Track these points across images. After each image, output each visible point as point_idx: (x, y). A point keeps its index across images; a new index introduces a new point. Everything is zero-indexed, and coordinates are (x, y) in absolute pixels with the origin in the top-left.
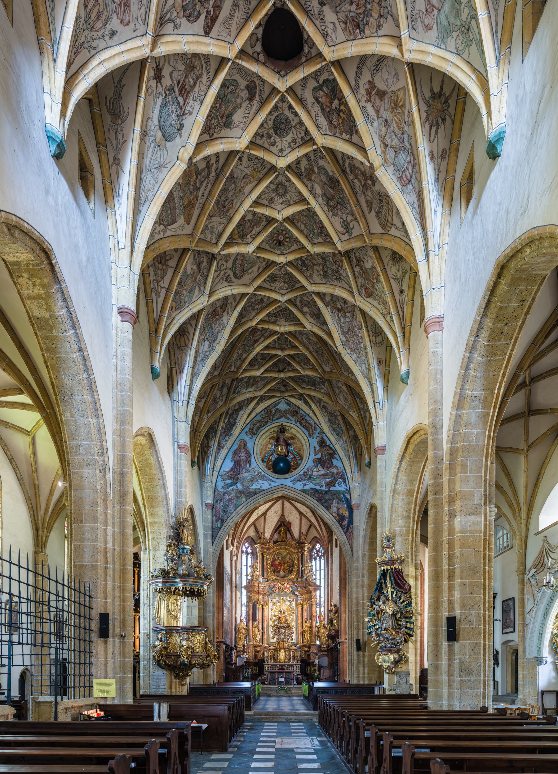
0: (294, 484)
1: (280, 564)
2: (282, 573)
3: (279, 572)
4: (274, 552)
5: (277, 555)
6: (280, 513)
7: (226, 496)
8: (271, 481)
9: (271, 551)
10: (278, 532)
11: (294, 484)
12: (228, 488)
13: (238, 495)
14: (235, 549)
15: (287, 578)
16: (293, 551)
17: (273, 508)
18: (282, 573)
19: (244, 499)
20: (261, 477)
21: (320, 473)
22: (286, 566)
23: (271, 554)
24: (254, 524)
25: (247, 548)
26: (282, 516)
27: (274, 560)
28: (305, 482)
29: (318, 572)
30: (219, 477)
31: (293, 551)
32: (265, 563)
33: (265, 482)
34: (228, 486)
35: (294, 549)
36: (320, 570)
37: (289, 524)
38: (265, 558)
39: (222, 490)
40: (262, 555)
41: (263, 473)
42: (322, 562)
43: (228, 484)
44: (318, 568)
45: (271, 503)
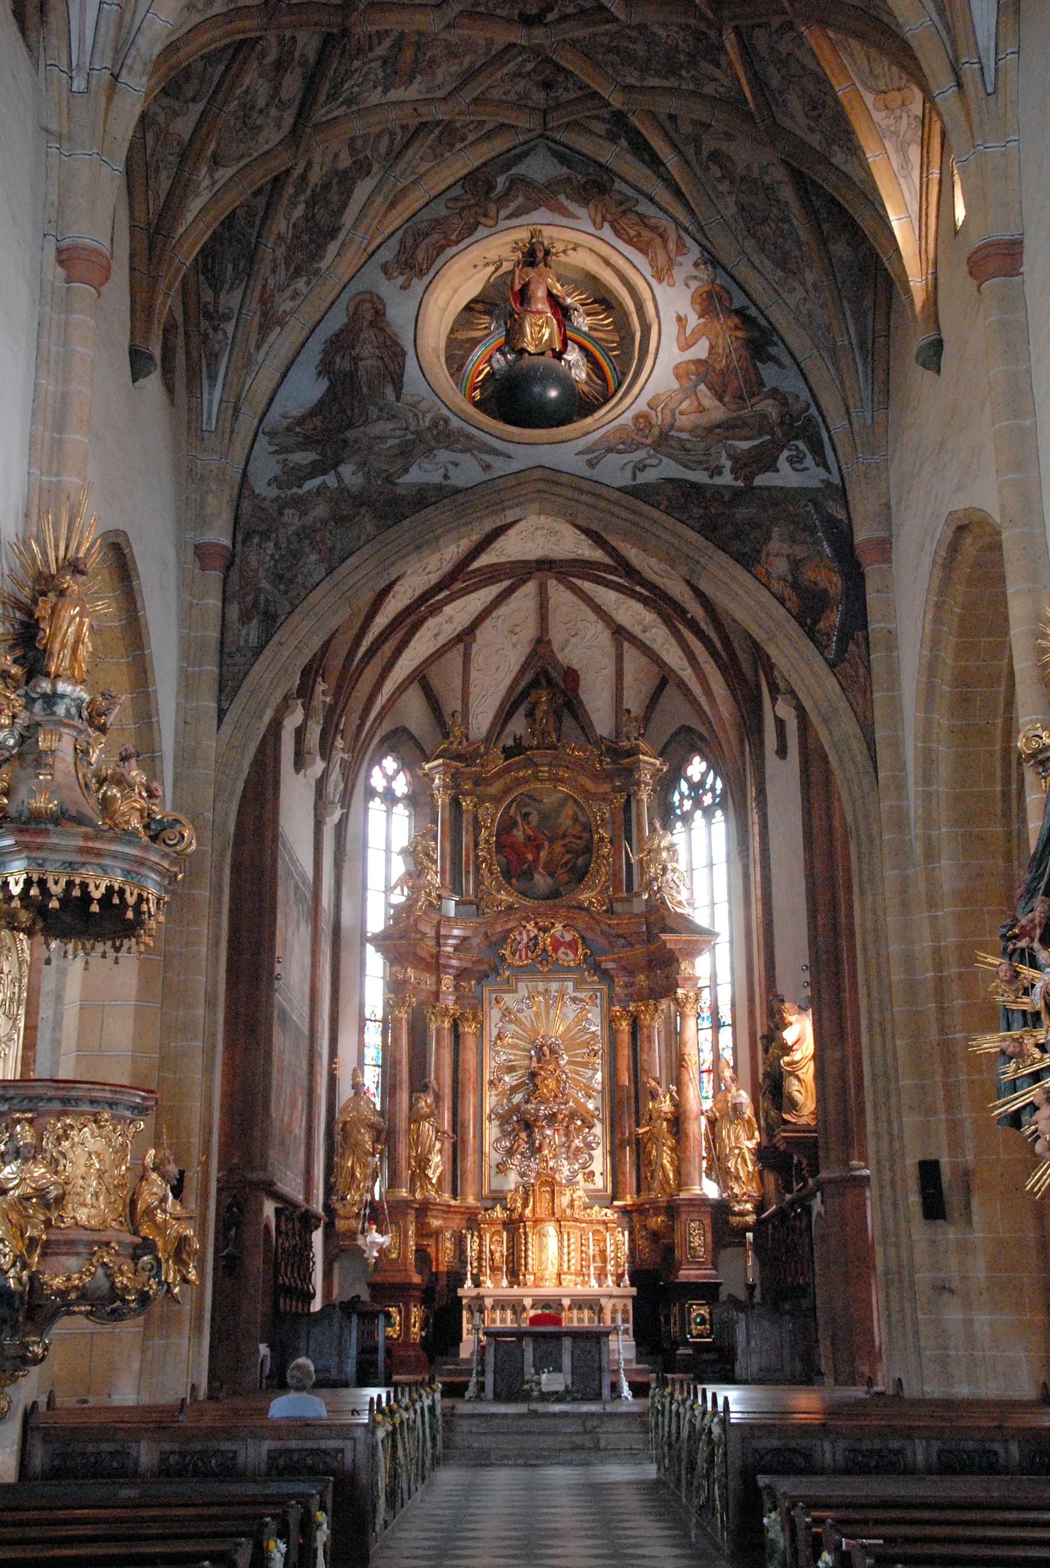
0: (591, 464)
2: (541, 881)
3: (528, 875)
4: (507, 791)
5: (520, 802)
6: (529, 632)
7: (290, 516)
9: (493, 790)
10: (522, 711)
11: (591, 464)
12: (300, 482)
13: (346, 510)
14: (335, 776)
15: (564, 901)
16: (589, 785)
17: (503, 610)
18: (541, 881)
19: (370, 528)
21: (704, 420)
22: (558, 849)
23: (496, 800)
24: (420, 677)
25: (390, 779)
26: (541, 643)
27: (506, 827)
28: (641, 454)
29: (701, 877)
30: (263, 440)
31: (589, 785)
32: (466, 839)
33: (465, 459)
34: (299, 475)
35: (595, 777)
36: (711, 865)
37: (572, 676)
38: (466, 820)
39: (272, 492)
40: (455, 803)
43: (299, 467)
44: (700, 860)
45: (494, 590)
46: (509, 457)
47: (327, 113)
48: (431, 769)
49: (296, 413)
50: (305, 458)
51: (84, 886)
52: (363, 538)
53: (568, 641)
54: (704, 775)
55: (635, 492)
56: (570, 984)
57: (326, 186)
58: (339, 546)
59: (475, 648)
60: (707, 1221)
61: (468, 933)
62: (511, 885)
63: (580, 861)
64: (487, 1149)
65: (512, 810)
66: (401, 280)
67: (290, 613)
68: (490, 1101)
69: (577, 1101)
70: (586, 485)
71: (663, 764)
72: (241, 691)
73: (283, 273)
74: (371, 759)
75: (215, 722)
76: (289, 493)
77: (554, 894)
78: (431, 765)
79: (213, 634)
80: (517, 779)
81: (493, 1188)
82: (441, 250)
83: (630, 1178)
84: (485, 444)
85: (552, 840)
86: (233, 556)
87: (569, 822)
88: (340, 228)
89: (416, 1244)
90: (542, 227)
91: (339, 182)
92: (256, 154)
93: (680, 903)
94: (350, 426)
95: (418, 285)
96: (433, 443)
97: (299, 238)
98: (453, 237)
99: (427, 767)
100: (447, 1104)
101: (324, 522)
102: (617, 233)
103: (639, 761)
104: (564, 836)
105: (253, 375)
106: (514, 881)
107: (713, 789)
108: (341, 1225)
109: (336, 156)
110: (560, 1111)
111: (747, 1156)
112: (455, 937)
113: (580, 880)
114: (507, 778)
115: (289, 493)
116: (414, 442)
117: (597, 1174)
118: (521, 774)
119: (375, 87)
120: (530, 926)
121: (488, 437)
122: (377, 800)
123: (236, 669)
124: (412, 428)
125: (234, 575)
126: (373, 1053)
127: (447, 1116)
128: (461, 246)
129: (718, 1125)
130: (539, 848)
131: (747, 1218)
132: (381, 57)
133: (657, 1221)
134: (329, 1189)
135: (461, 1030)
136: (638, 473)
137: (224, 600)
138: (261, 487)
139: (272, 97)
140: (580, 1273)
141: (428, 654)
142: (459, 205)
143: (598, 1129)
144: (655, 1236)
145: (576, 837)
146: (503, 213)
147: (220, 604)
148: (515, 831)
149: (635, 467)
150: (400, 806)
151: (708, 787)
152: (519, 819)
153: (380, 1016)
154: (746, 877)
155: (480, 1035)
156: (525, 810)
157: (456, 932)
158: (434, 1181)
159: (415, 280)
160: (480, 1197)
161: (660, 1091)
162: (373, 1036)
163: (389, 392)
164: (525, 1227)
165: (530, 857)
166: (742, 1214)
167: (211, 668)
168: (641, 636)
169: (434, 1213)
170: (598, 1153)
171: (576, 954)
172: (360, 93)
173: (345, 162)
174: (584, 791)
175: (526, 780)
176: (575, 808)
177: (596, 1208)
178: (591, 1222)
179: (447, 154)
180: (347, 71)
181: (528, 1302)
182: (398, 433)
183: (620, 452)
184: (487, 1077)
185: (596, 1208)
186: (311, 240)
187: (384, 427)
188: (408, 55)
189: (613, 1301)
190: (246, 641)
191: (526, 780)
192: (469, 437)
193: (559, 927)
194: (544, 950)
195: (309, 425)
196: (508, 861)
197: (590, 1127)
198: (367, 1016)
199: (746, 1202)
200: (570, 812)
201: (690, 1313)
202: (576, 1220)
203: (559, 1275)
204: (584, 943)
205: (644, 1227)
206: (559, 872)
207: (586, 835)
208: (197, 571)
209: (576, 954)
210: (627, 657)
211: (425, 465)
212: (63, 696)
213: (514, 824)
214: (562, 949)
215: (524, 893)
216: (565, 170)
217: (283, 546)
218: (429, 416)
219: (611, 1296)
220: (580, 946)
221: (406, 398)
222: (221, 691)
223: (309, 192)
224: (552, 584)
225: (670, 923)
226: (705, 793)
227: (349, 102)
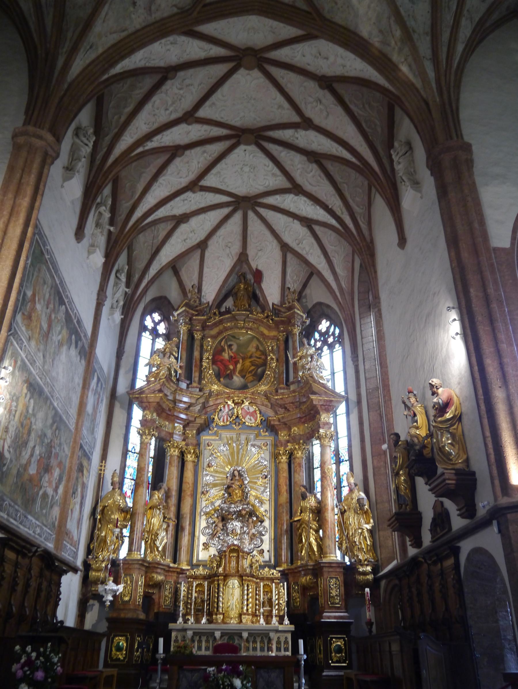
1: (234, 360)
2: (237, 380)
3: (230, 377)
4: (220, 333)
6: (236, 248)
9: (214, 332)
16: (266, 332)
17: (222, 232)
18: (237, 380)
22: (248, 363)
23: (214, 337)
25: (156, 324)
27: (218, 352)
31: (266, 332)
32: (196, 354)
35: (269, 328)
37: (258, 275)
38: (197, 344)
42: (338, 350)
48: (178, 315)
53: (257, 254)
54: (328, 328)
56: (252, 437)
59: (207, 254)
60: (341, 578)
61: (193, 401)
62: (219, 381)
63: (260, 370)
64: (197, 534)
65: (223, 343)
68: (203, 504)
69: (253, 506)
71: (307, 318)
74: (145, 309)
77: (244, 387)
78: (178, 312)
80: (225, 327)
81: (200, 558)
83: (284, 554)
85: (244, 359)
87: (254, 350)
89: (144, 592)
93: (322, 377)
99: (176, 314)
100: (173, 501)
103: (295, 312)
104: (251, 357)
106: (222, 379)
107: (333, 334)
108: (93, 574)
110: (243, 509)
111: (366, 534)
112: (185, 403)
113: (259, 380)
114: (221, 327)
117: (266, 551)
118: (229, 324)
120: (230, 403)
122: (148, 333)
126: (131, 472)
127: (173, 509)
129: (346, 515)
130: (236, 363)
131: (368, 577)
133: (305, 580)
134: (89, 551)
135: (185, 459)
140: (254, 615)
141: (180, 252)
143: (266, 523)
144: (305, 589)
145: (257, 358)
148: (223, 353)
150: (161, 339)
151: (330, 333)
152: (226, 348)
153: (138, 450)
154: (357, 372)
155: (196, 465)
156: (229, 343)
157: (185, 399)
158: (160, 549)
160: (190, 562)
161: (308, 494)
162: (132, 462)
164: (218, 580)
165: (231, 367)
166: (365, 573)
168: (297, 248)
169: (159, 570)
170: (266, 538)
171: (256, 420)
174: (262, 334)
175: (231, 328)
176: (258, 343)
177: (267, 569)
178: (262, 579)
181: (218, 634)
184: (200, 490)
185: (267, 569)
189: (278, 635)
191: (231, 328)
193: (247, 403)
194: (237, 417)
196: (219, 369)
197: (262, 521)
198: (130, 448)
199: (367, 565)
200: (255, 345)
201: (331, 644)
202: (253, 576)
203: (240, 615)
204: (260, 413)
205: (296, 583)
206: (247, 376)
207: (263, 357)
209: (256, 420)
210: (288, 264)
213: (223, 350)
214: (248, 416)
215: (227, 386)
219: (277, 631)
220: (259, 415)
224: (251, 215)
225: (315, 387)
226: (329, 337)
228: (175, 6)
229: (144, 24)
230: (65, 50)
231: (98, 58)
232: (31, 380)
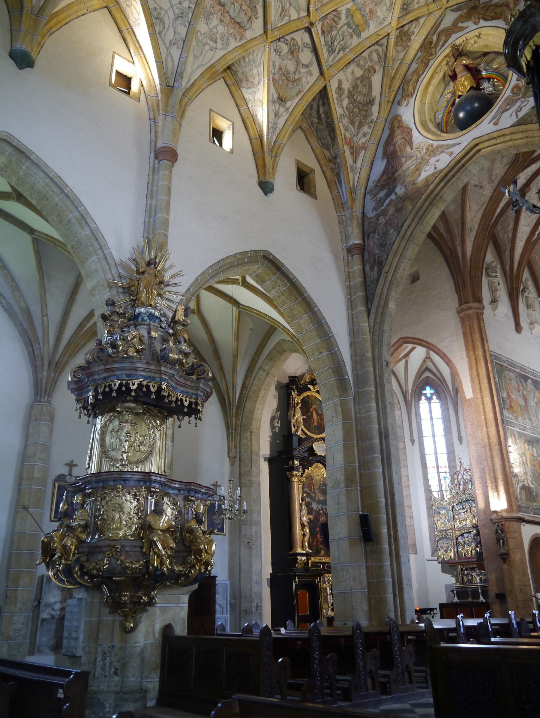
8: (453, 145)
11: (496, 124)
20: (432, 151)
30: (368, 196)
34: (381, 202)
39: (375, 213)
41: (435, 144)
43: (381, 199)
46: (459, 144)
47: (334, 59)
49: (377, 179)
50: (382, 194)
51: (110, 386)
52: (408, 213)
55: (521, 122)
57: (355, 87)
58: (400, 221)
66: (405, 103)
67: (387, 258)
70: (495, 135)
72: (375, 298)
73: (353, 129)
75: (365, 315)
76: (379, 210)
79: (359, 280)
82: (418, 80)
84: (447, 145)
86: (364, 246)
88: (374, 100)
90: (454, 43)
91: (361, 82)
92: (305, 90)
94: (396, 171)
95: (412, 100)
96: (428, 158)
97: (352, 112)
98: (421, 73)
101: (393, 215)
102: (486, 20)
105: (358, 174)
109: (353, 73)
115: (379, 210)
116: (420, 162)
119: (352, 37)
121: (450, 141)
123: (372, 290)
124: (419, 157)
125: (366, 254)
128: (425, 74)
132: (345, 24)
136: (519, 114)
137: (364, 266)
138: (370, 214)
139: (297, 65)
142: (421, 59)
146: (438, 49)
147: (360, 267)
149: (516, 111)
159: (410, 99)
163: (408, 149)
167: (360, 294)
172: (345, 43)
173: (359, 73)
179: (409, 44)
180: (331, 39)
182: (414, 162)
183: (508, 110)
186: (360, 111)
187: (409, 163)
188: (358, 16)
190: (374, 277)
192: (442, 146)
195: (382, 180)
208: (350, 258)
211: (427, 169)
212: (140, 314)
216: (459, 13)
217: (381, 232)
218: (425, 148)
221: (414, 147)
222: (367, 302)
223: (346, 92)
227: (343, 49)
228: (506, 165)
229: (493, 191)
230: (458, 242)
231: (477, 232)
232: (528, 439)
